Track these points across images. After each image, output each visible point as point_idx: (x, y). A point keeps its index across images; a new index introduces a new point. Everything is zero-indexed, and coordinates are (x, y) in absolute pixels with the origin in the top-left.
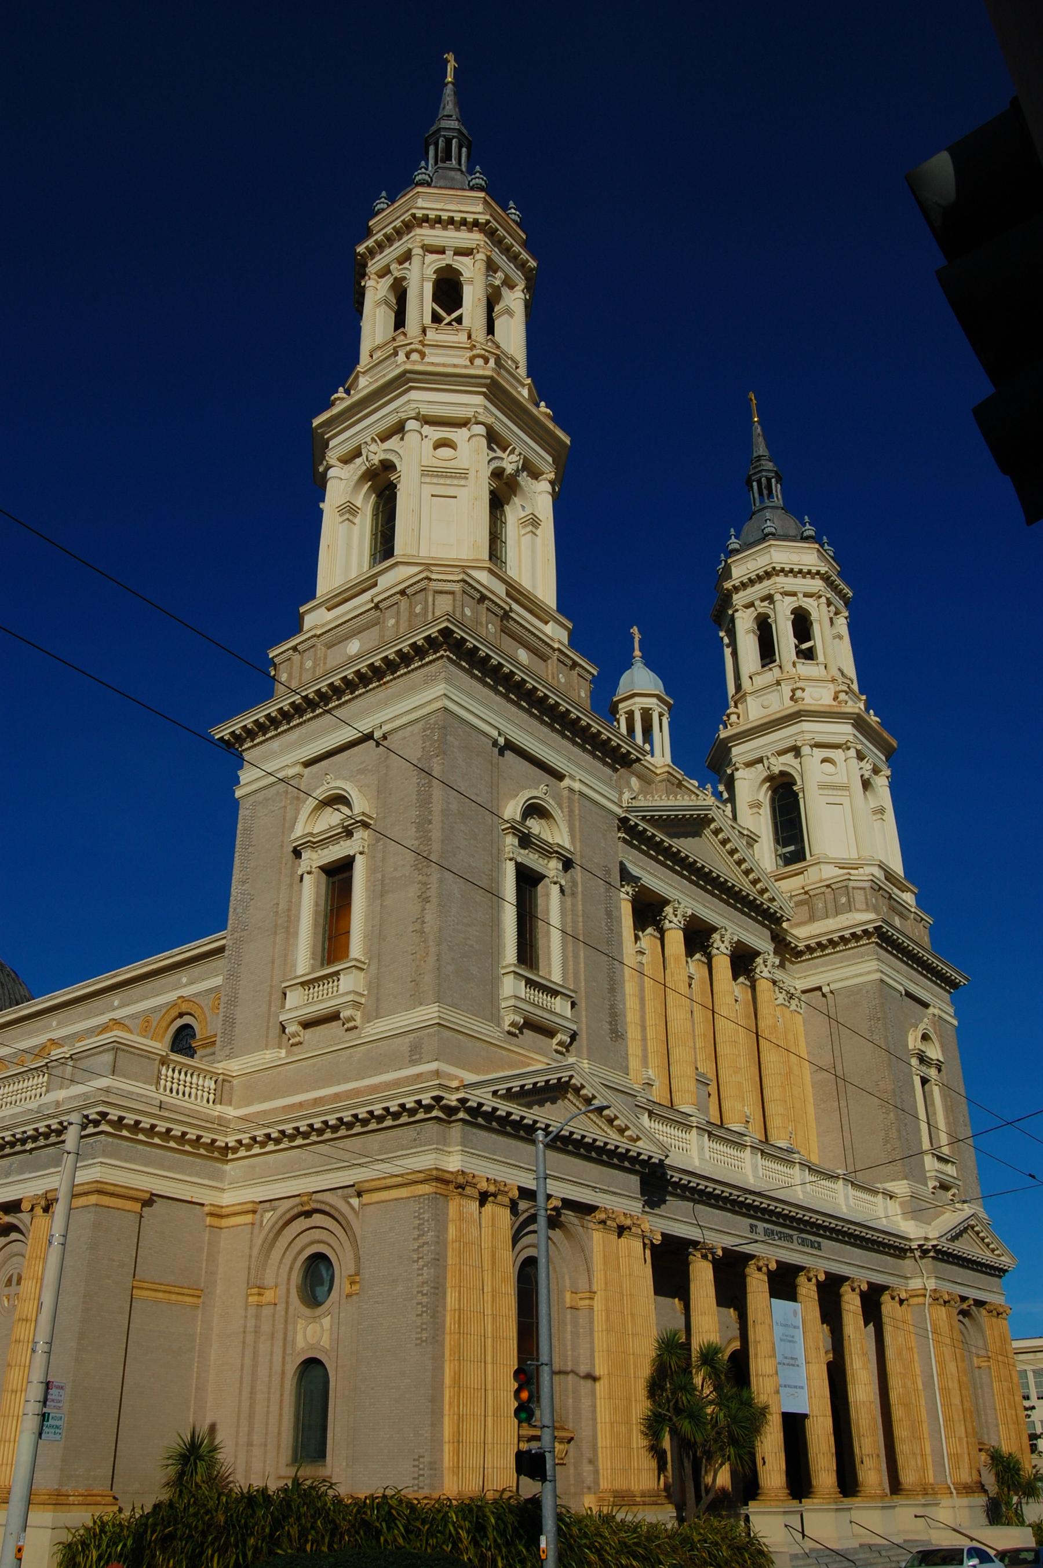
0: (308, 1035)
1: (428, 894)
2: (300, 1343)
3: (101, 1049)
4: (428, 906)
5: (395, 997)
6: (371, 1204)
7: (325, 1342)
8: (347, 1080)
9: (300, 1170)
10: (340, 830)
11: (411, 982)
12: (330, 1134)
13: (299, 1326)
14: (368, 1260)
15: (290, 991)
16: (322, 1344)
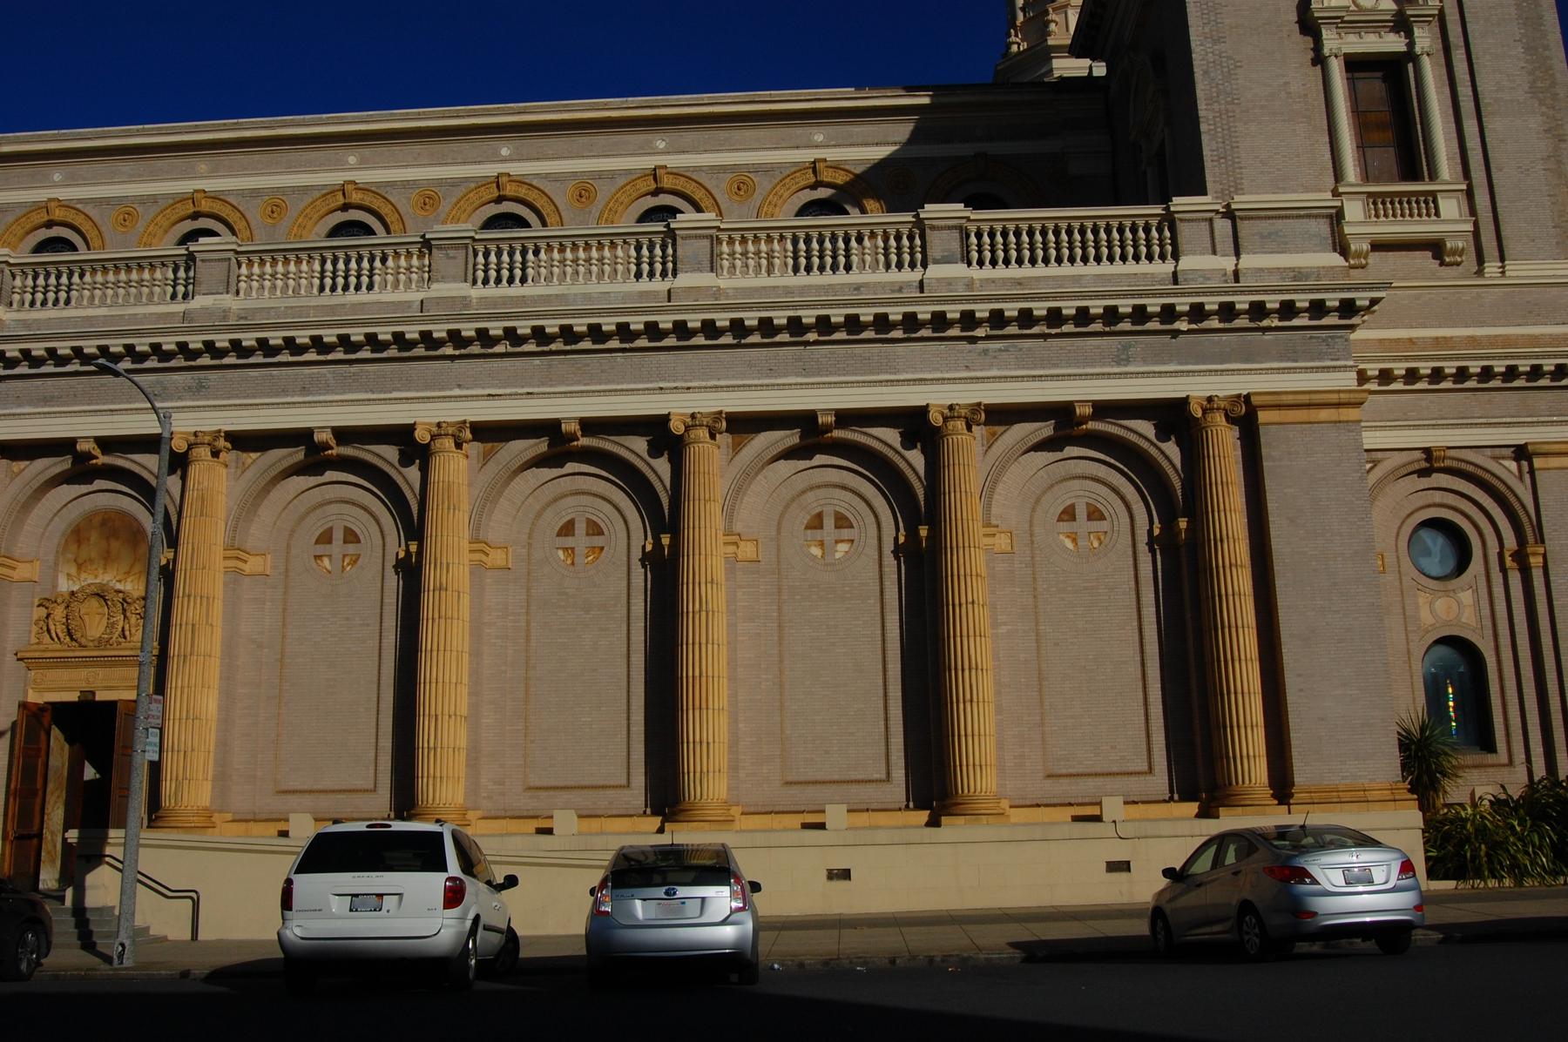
0: (1374, 258)
1: (1561, 132)
2: (1426, 617)
3: (1302, 212)
4: (1563, 145)
5: (1533, 241)
6: (1549, 469)
7: (1468, 617)
8: (1482, 324)
9: (1419, 420)
10: (1388, 18)
11: (1554, 227)
12: (1500, 382)
13: (1421, 601)
14: (1556, 531)
15: (1347, 200)
16: (1464, 620)
